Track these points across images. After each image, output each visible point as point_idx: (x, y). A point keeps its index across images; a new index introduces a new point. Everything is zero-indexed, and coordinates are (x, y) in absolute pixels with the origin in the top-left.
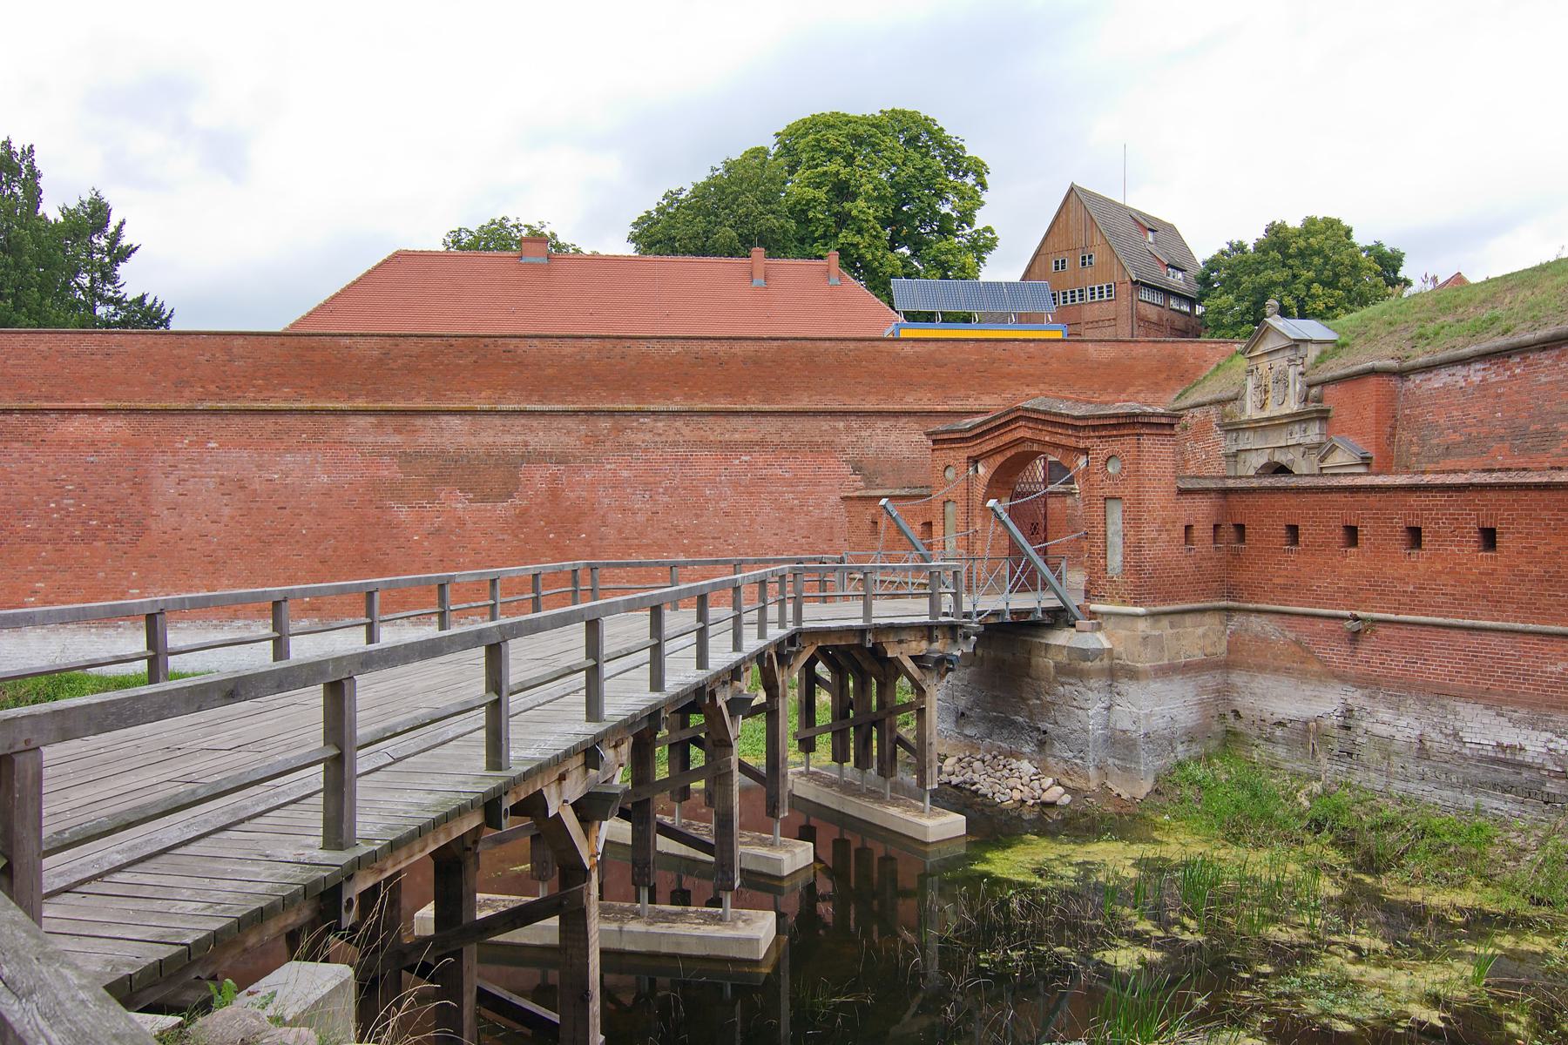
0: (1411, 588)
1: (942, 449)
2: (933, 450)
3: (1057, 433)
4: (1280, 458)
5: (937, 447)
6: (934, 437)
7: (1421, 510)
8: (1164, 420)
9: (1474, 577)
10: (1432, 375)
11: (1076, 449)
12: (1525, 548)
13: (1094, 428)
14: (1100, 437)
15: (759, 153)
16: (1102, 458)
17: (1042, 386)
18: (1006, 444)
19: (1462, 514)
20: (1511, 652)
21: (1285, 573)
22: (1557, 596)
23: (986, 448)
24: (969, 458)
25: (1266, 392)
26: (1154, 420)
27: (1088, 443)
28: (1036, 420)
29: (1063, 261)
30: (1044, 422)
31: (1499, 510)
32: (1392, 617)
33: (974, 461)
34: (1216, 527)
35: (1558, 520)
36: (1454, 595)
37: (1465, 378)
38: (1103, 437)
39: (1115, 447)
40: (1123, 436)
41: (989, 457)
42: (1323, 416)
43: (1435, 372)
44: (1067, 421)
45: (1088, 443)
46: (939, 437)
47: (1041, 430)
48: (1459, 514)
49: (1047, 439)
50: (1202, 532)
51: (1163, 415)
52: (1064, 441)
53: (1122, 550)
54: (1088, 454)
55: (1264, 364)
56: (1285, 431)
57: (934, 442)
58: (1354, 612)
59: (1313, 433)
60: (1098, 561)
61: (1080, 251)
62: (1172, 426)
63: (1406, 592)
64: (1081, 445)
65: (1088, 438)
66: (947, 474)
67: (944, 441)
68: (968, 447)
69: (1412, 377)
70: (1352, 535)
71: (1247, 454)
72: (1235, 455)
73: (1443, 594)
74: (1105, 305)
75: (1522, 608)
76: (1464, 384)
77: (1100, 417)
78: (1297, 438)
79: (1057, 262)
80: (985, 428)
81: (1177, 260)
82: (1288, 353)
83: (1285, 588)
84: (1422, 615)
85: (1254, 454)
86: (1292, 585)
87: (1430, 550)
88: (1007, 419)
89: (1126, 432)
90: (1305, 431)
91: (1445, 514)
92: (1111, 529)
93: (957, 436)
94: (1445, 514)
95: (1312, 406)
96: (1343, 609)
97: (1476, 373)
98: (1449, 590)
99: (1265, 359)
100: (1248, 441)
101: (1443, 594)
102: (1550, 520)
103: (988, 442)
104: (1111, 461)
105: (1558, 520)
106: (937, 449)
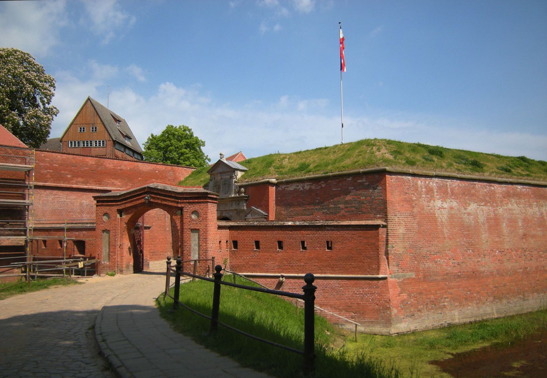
0: (302, 264)
2: (97, 206)
5: (99, 204)
7: (307, 235)
8: (215, 197)
9: (325, 259)
10: (289, 186)
12: (342, 248)
14: (188, 203)
19: (320, 236)
20: (338, 285)
21: (254, 260)
22: (352, 264)
23: (128, 205)
24: (118, 210)
27: (183, 205)
29: (84, 128)
31: (333, 234)
35: (352, 238)
36: (318, 266)
37: (303, 187)
39: (196, 207)
40: (200, 202)
43: (291, 185)
48: (319, 236)
57: (98, 202)
60: (187, 257)
61: (92, 125)
63: (301, 265)
69: (281, 186)
70: (280, 245)
73: (314, 266)
74: (101, 149)
75: (341, 269)
79: (81, 128)
81: (130, 135)
83: (254, 266)
87: (309, 249)
91: (314, 236)
94: (315, 236)
97: (307, 187)
98: (316, 264)
102: (349, 238)
105: (352, 238)
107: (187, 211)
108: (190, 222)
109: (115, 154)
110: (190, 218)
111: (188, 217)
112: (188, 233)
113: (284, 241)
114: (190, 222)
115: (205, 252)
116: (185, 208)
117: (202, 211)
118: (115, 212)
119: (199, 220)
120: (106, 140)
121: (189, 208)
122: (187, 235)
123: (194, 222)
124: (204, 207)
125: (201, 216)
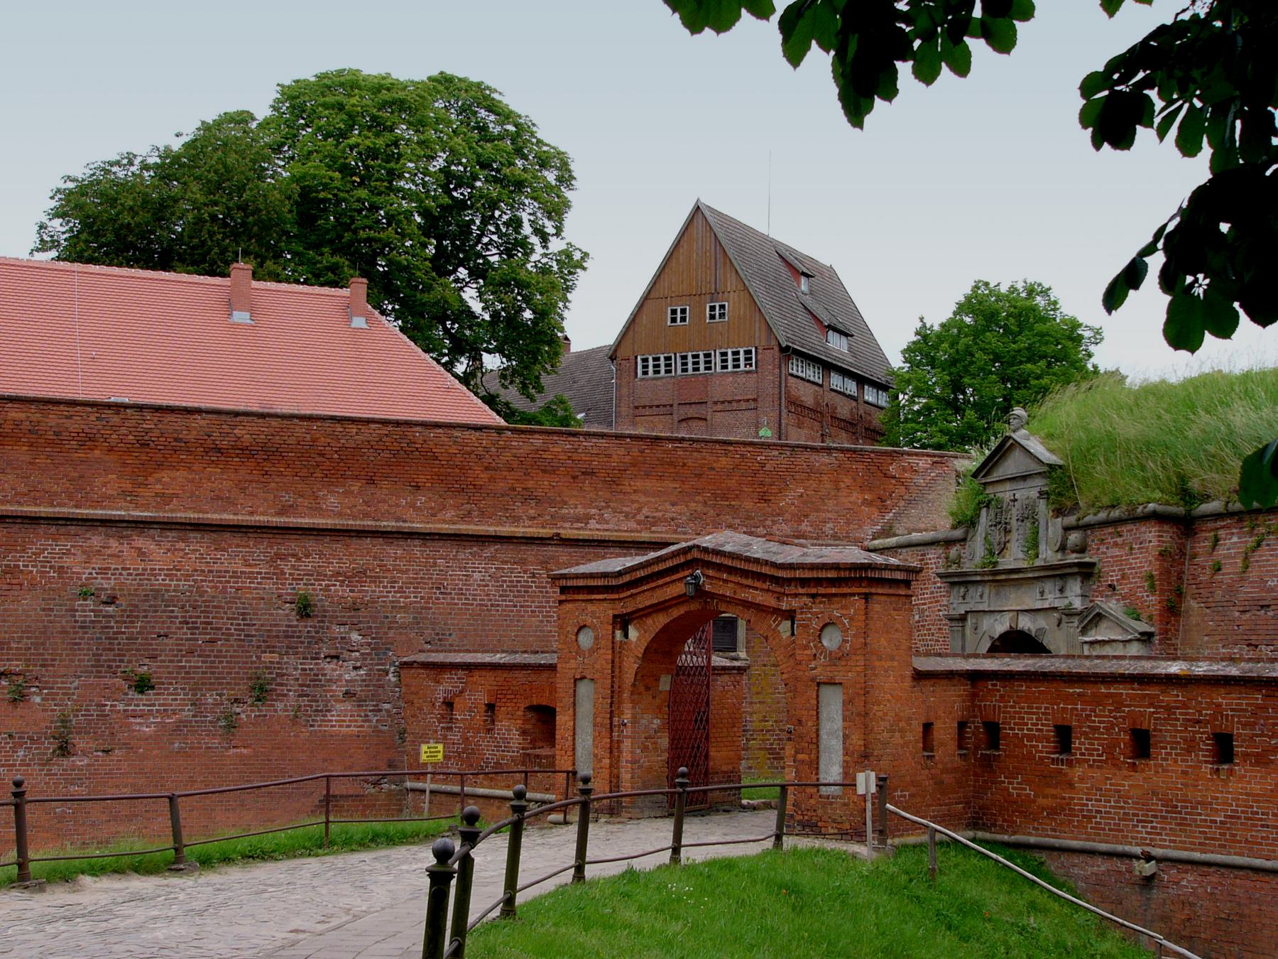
3: (750, 587)
4: (1025, 623)
6: (563, 583)
11: (777, 611)
13: (804, 582)
15: (242, 118)
16: (816, 625)
25: (1007, 532)
26: (887, 575)
27: (795, 603)
28: (719, 567)
30: (731, 570)
32: (1197, 855)
33: (622, 622)
34: (962, 725)
40: (844, 595)
42: (1086, 572)
44: (766, 570)
45: (795, 603)
46: (570, 583)
47: (725, 581)
50: (945, 732)
51: (898, 568)
52: (760, 598)
53: (841, 758)
55: (1005, 493)
56: (1037, 588)
57: (564, 590)
58: (1147, 849)
59: (1074, 596)
61: (708, 297)
62: (907, 584)
65: (796, 595)
66: (581, 637)
67: (578, 589)
68: (620, 599)
72: (963, 618)
74: (742, 379)
77: (813, 567)
78: (1052, 599)
79: (674, 312)
81: (842, 320)
82: (1039, 482)
84: (1236, 854)
90: (1061, 591)
92: (826, 727)
93: (600, 582)
95: (1073, 558)
96: (1131, 844)
99: (1008, 486)
100: (979, 599)
101: (1263, 826)
104: (828, 630)
106: (566, 601)
109: (788, 393)
113: (1155, 730)
120: (756, 348)
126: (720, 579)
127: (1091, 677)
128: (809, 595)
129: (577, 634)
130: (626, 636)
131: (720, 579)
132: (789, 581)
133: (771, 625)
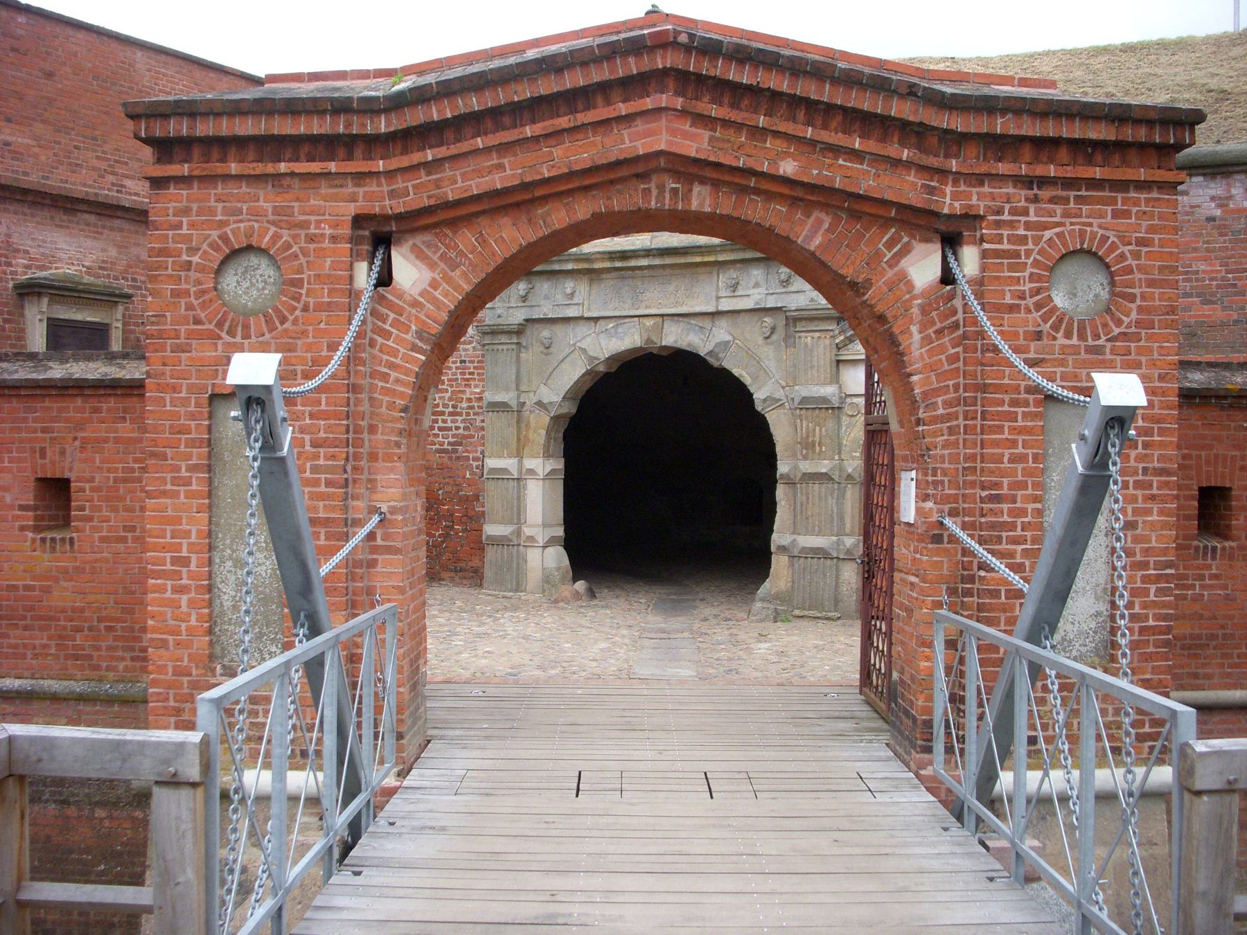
1: (209, 179)
2: (158, 183)
3: (835, 150)
6: (178, 127)
14: (1027, 182)
17: (39, 128)
18: (571, 175)
24: (359, 221)
27: (977, 199)
37: (1222, 202)
38: (1044, 182)
40: (1121, 186)
41: (453, 223)
45: (977, 199)
49: (788, 168)
52: (868, 180)
54: (951, 242)
56: (724, 279)
64: (949, 202)
65: (980, 179)
66: (230, 281)
68: (360, 177)
71: (559, 330)
76: (1218, 212)
80: (474, 103)
85: (582, 329)
86: (1213, 637)
88: (597, 75)
89: (1142, 174)
93: (317, 126)
103: (471, 165)
107: (1017, 255)
108: (1038, 336)
110: (1038, 306)
111: (1022, 296)
112: (1021, 430)
114: (1038, 336)
115: (1158, 578)
116: (998, 224)
117: (1136, 255)
118: (334, 239)
119: (1119, 323)
121: (1028, 226)
122: (1013, 443)
123: (1075, 341)
124: (1151, 229)
125: (1132, 298)
126: (739, 127)
127: (1225, 397)
128: (1018, 180)
129: (219, 272)
130: (385, 279)
131: (739, 127)
132: (954, 141)
133: (878, 255)
